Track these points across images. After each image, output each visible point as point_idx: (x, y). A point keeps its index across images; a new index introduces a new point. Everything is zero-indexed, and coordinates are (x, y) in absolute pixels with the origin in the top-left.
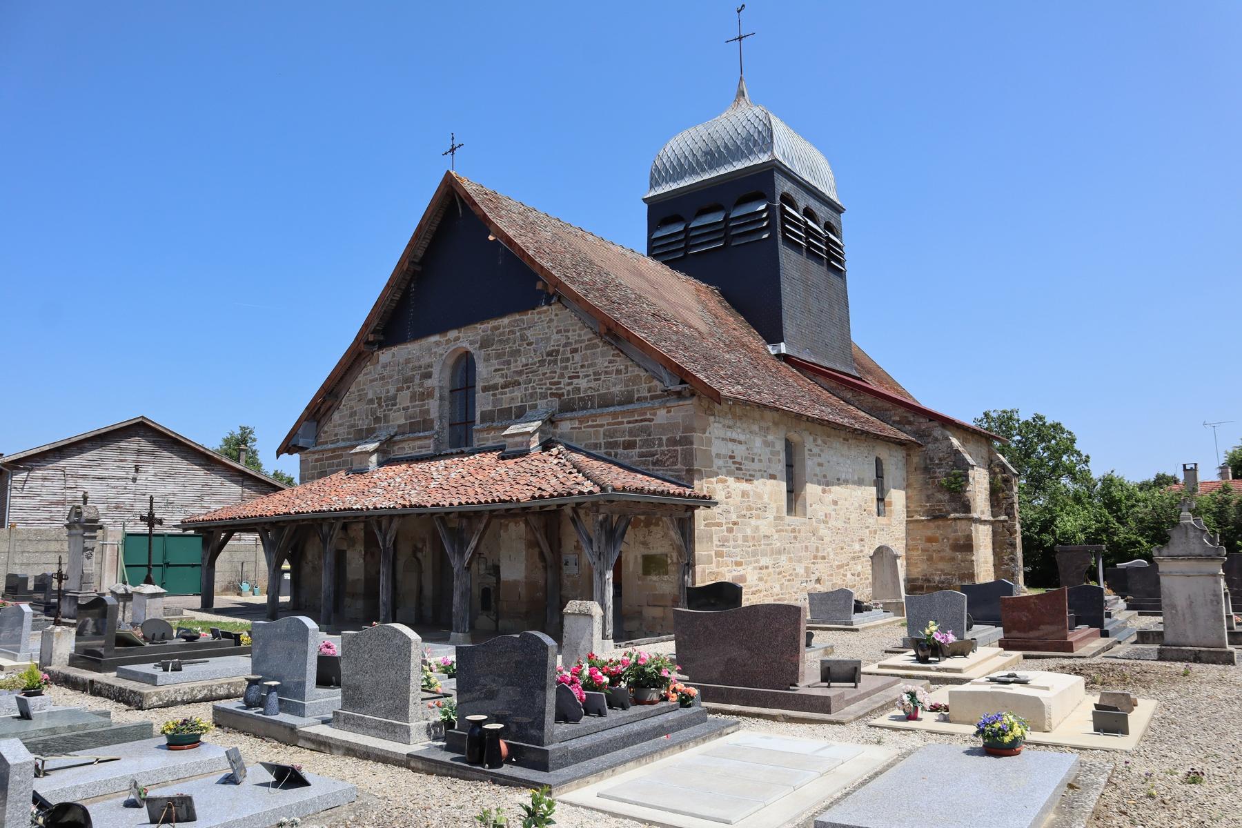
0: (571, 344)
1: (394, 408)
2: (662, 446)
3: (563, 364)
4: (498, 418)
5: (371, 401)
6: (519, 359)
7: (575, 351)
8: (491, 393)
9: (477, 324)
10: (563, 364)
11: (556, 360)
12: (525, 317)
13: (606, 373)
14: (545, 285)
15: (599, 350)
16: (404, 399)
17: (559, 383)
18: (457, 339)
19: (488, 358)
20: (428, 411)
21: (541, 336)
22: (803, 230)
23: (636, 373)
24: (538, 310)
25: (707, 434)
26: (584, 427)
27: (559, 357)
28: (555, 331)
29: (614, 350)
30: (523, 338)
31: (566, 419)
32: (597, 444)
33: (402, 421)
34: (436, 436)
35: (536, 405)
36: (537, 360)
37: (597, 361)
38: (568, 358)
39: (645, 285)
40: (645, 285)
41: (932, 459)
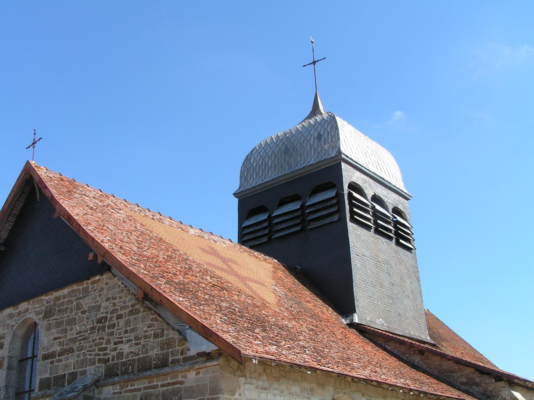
0: (116, 310)
3: (110, 330)
4: (54, 385)
6: (74, 327)
7: (120, 317)
8: (50, 360)
9: (42, 295)
10: (110, 330)
11: (104, 327)
12: (81, 288)
13: (146, 337)
14: (96, 256)
15: (140, 315)
17: (106, 349)
18: (27, 310)
19: (49, 328)
21: (93, 304)
23: (171, 336)
24: (92, 280)
25: (237, 396)
26: (125, 392)
27: (107, 324)
28: (104, 299)
29: (153, 315)
30: (78, 307)
31: (108, 385)
35: (86, 371)
36: (88, 327)
37: (138, 326)
38: (114, 324)
39: (218, 262)
40: (218, 262)
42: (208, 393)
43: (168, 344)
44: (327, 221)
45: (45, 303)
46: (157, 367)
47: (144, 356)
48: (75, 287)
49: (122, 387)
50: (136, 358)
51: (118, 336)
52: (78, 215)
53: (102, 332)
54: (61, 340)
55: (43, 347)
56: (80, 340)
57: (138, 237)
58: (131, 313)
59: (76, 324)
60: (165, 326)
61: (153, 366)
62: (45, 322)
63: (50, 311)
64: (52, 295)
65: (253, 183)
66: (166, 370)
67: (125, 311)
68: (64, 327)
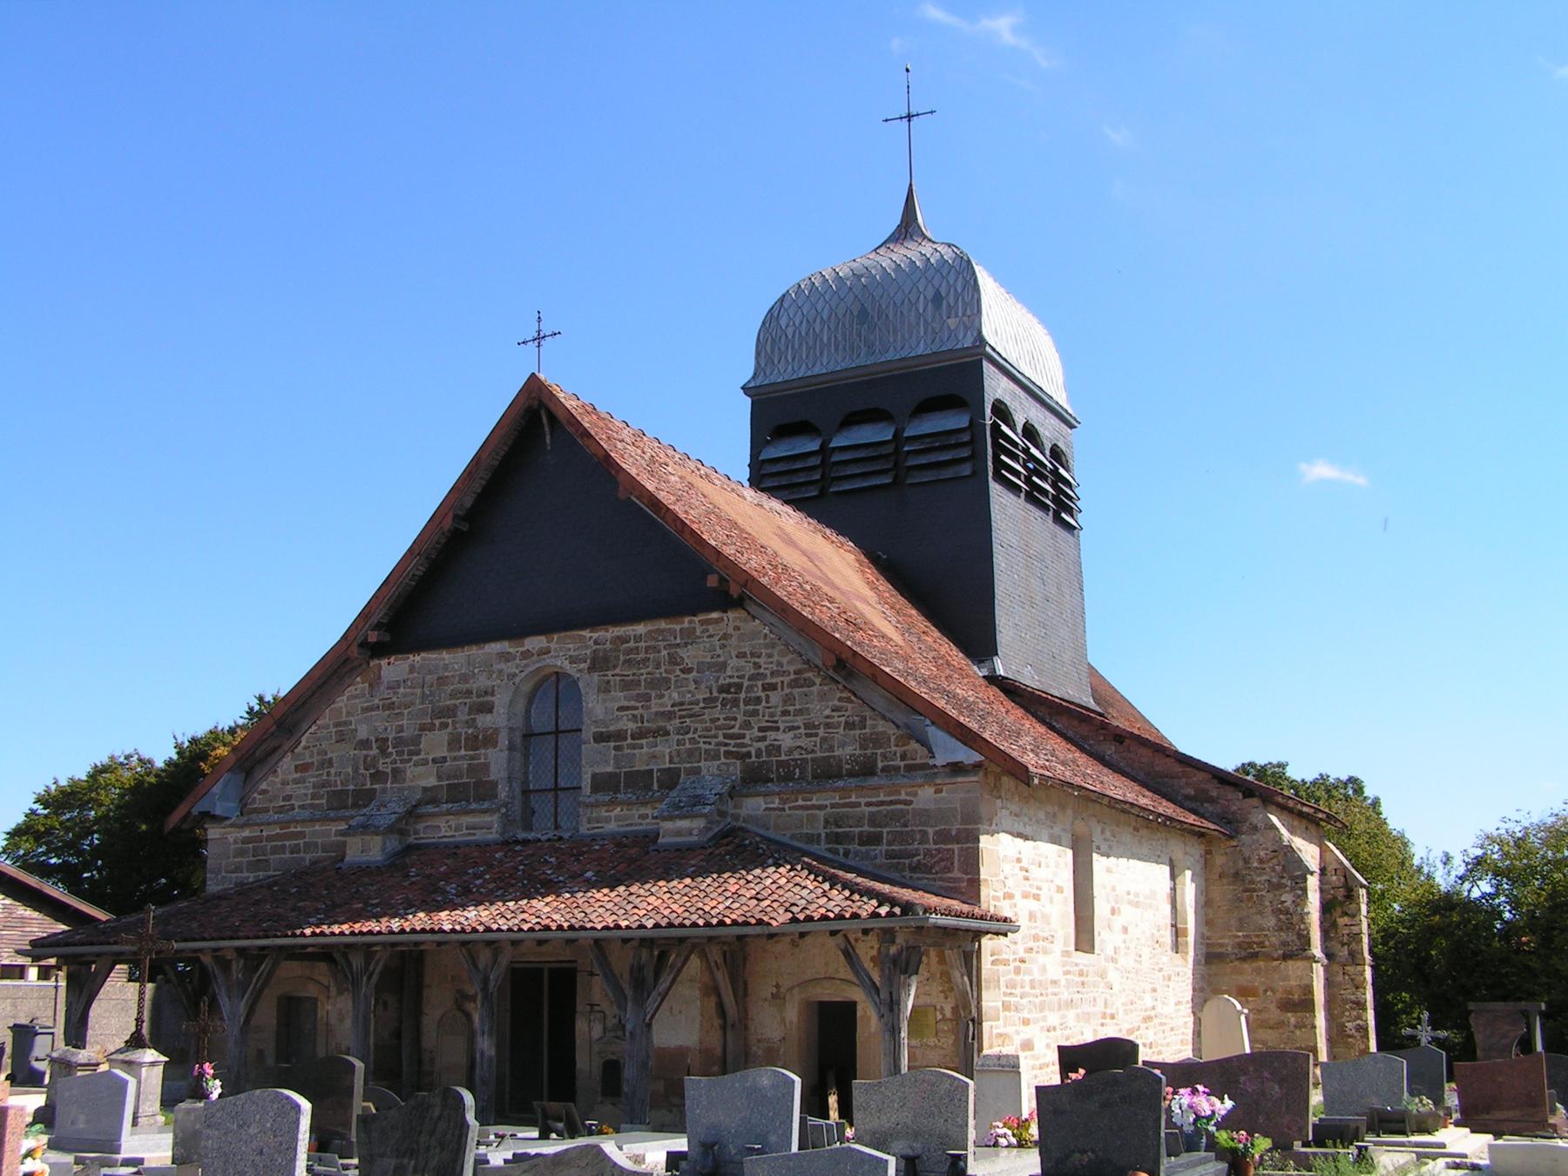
0: (764, 676)
1: (415, 758)
2: (927, 842)
3: (751, 708)
5: (365, 744)
10: (751, 708)
12: (678, 627)
13: (828, 726)
14: (722, 580)
15: (815, 689)
18: (545, 652)
19: (605, 688)
20: (486, 766)
21: (708, 660)
22: (1050, 481)
23: (880, 729)
26: (790, 808)
27: (743, 695)
28: (734, 653)
29: (842, 692)
30: (673, 660)
31: (758, 795)
32: (813, 835)
33: (432, 781)
34: (504, 810)
36: (700, 697)
41: (1246, 861)
42: (959, 820)
43: (878, 740)
44: (948, 473)
45: (592, 642)
46: (851, 774)
47: (827, 754)
48: (663, 624)
49: (784, 801)
51: (766, 718)
53: (731, 708)
54: (635, 712)
55: (594, 719)
58: (794, 684)
59: (669, 688)
60: (868, 713)
61: (844, 772)
63: (606, 659)
64: (607, 631)
65: (784, 373)
66: (874, 781)
67: (781, 679)
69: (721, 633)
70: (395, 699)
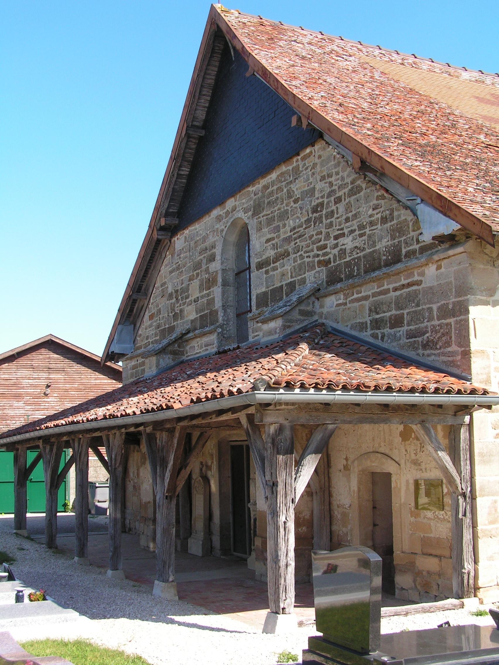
0: (334, 191)
1: (187, 300)
2: (433, 319)
3: (329, 221)
4: (272, 301)
5: (170, 296)
6: (287, 222)
7: (338, 200)
8: (264, 269)
9: (248, 186)
10: (329, 221)
11: (321, 217)
12: (290, 168)
13: (372, 224)
14: (299, 119)
15: (362, 194)
16: (195, 292)
17: (325, 247)
18: (234, 209)
21: (306, 188)
23: (403, 218)
24: (302, 155)
27: (324, 212)
28: (319, 178)
29: (378, 191)
32: (362, 323)
34: (220, 330)
36: (303, 220)
37: (361, 209)
38: (332, 212)
42: (454, 294)
46: (388, 264)
47: (371, 250)
48: (284, 168)
49: (346, 296)
50: (361, 254)
51: (338, 227)
52: (279, 67)
53: (319, 224)
54: (274, 242)
55: (255, 252)
56: (295, 239)
57: (373, 90)
59: (288, 218)
60: (395, 205)
61: (382, 264)
62: (255, 220)
63: (259, 205)
64: (259, 184)
66: (399, 266)
67: (344, 191)
68: (276, 224)
69: (312, 164)
70: (180, 262)
